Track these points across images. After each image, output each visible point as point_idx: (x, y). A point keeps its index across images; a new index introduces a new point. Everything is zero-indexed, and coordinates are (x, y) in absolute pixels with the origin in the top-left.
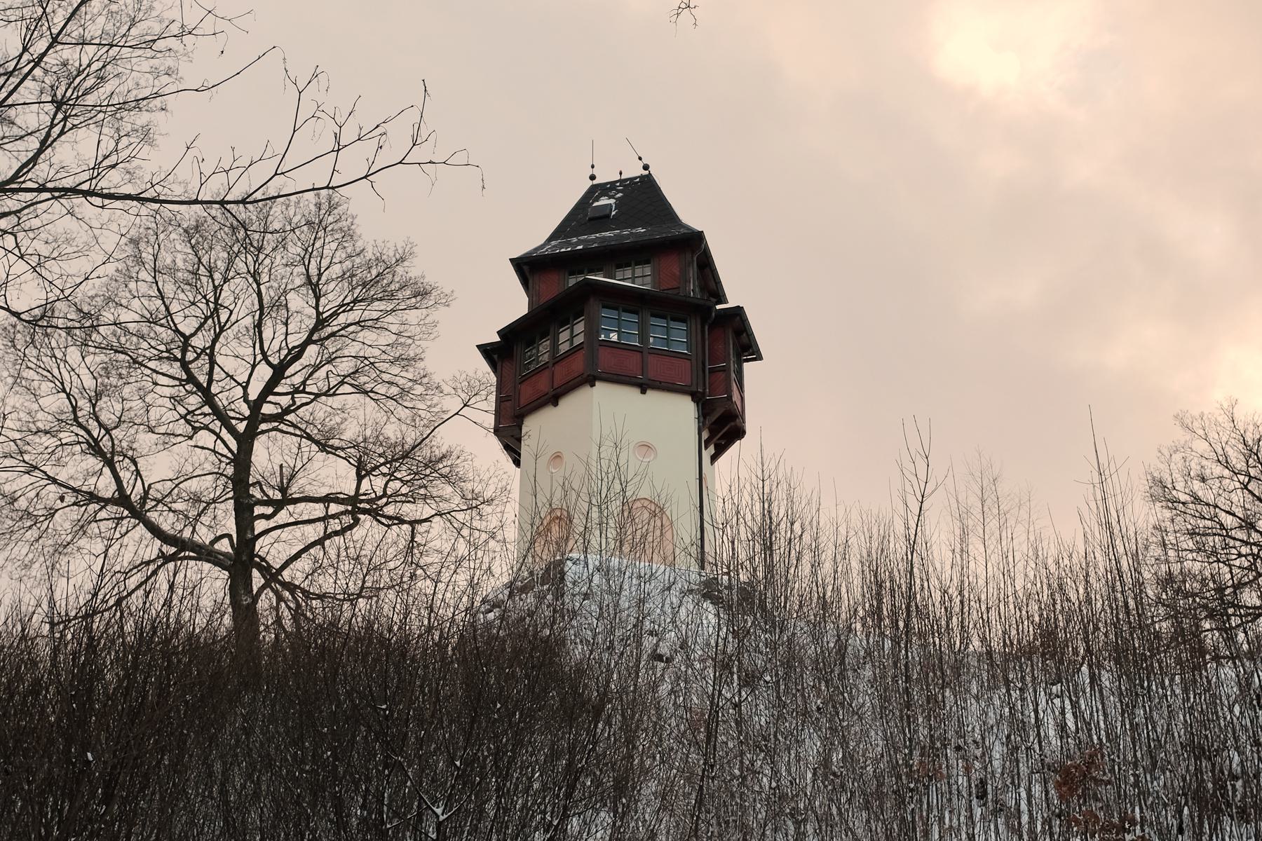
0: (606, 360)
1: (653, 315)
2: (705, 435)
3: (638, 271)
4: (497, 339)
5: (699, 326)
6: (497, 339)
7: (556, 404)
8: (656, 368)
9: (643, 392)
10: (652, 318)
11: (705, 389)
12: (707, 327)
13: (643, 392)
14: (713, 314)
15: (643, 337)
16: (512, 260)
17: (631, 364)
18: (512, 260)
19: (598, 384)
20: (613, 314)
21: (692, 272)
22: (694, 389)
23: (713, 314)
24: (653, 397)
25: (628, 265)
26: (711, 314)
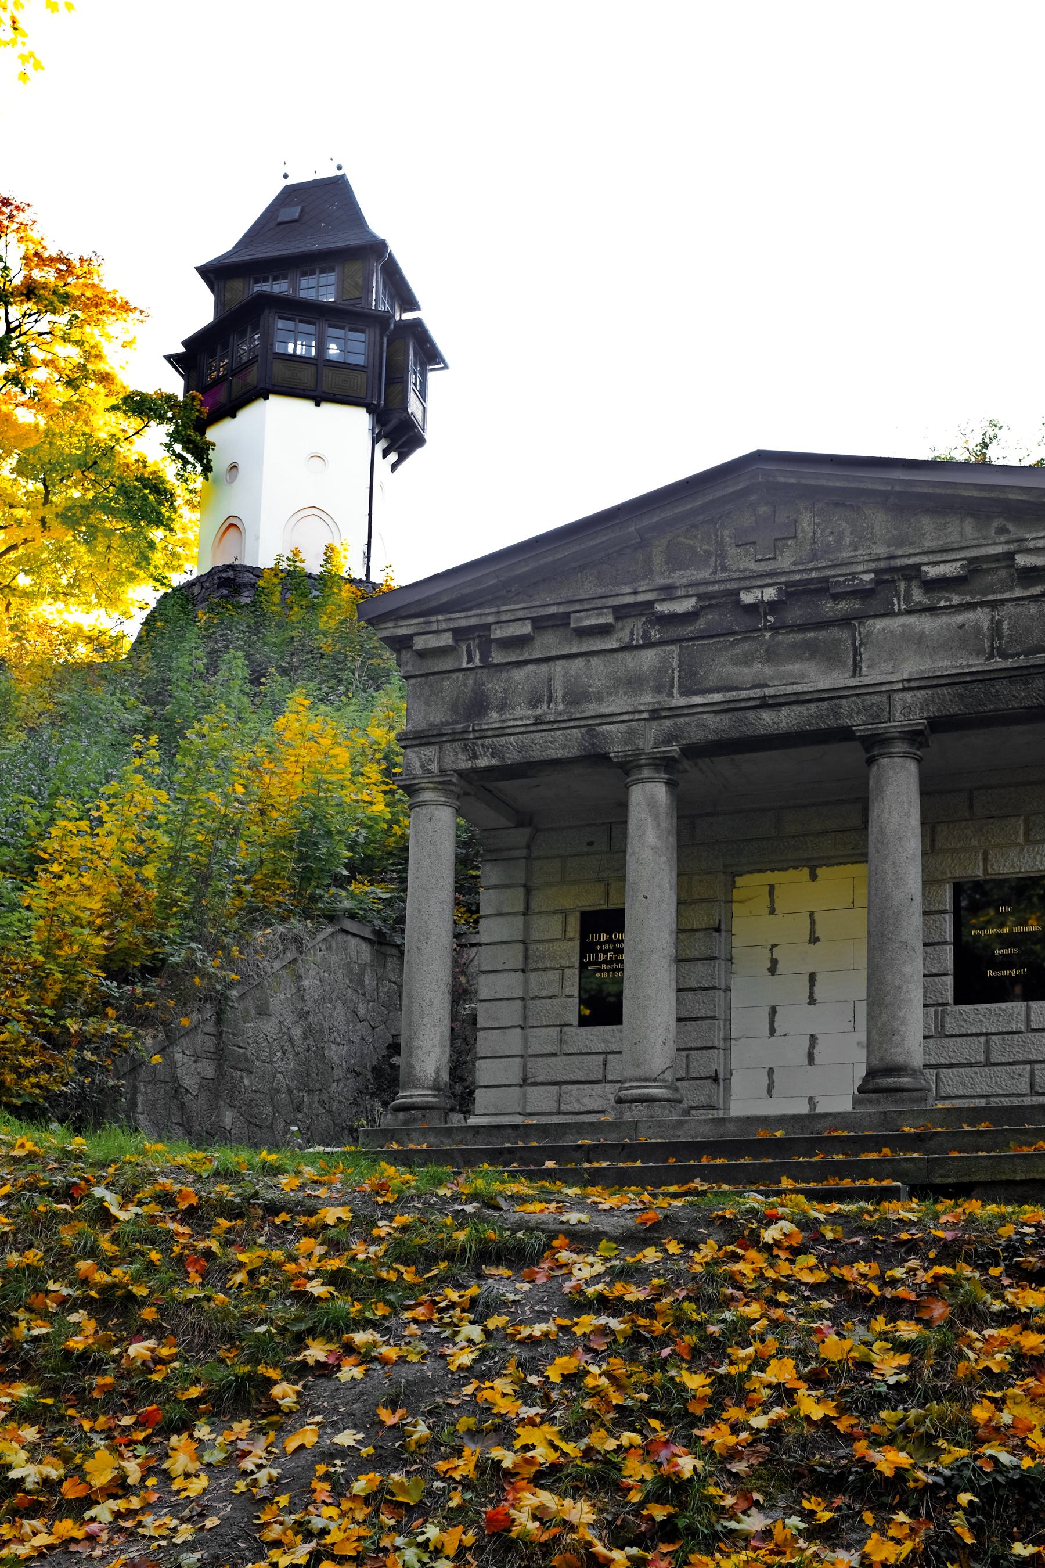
0: (279, 371)
1: (330, 326)
2: (379, 448)
3: (323, 281)
4: (183, 350)
5: (378, 339)
6: (183, 350)
7: (234, 416)
8: (330, 380)
9: (318, 404)
10: (330, 329)
11: (379, 404)
12: (385, 339)
13: (318, 404)
14: (392, 326)
15: (321, 348)
16: (197, 269)
17: (306, 376)
18: (197, 269)
19: (272, 397)
20: (290, 325)
21: (376, 281)
22: (366, 401)
23: (392, 326)
24: (329, 409)
25: (313, 273)
26: (389, 325)
